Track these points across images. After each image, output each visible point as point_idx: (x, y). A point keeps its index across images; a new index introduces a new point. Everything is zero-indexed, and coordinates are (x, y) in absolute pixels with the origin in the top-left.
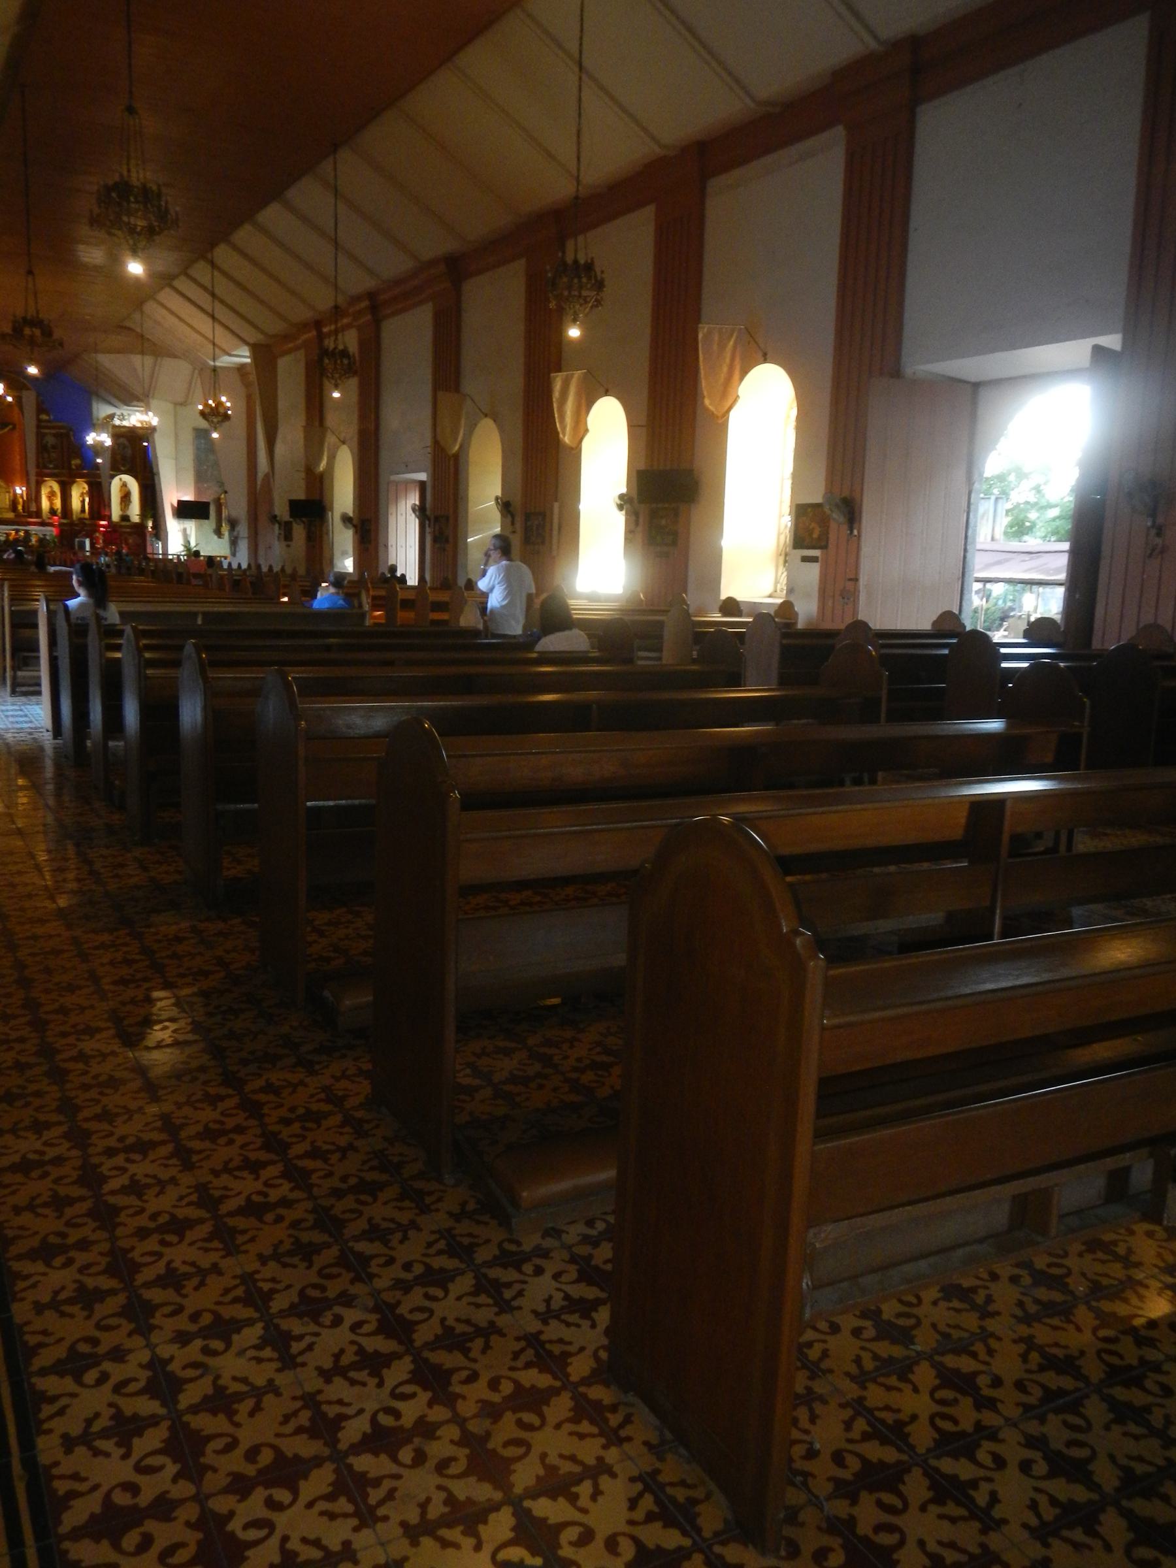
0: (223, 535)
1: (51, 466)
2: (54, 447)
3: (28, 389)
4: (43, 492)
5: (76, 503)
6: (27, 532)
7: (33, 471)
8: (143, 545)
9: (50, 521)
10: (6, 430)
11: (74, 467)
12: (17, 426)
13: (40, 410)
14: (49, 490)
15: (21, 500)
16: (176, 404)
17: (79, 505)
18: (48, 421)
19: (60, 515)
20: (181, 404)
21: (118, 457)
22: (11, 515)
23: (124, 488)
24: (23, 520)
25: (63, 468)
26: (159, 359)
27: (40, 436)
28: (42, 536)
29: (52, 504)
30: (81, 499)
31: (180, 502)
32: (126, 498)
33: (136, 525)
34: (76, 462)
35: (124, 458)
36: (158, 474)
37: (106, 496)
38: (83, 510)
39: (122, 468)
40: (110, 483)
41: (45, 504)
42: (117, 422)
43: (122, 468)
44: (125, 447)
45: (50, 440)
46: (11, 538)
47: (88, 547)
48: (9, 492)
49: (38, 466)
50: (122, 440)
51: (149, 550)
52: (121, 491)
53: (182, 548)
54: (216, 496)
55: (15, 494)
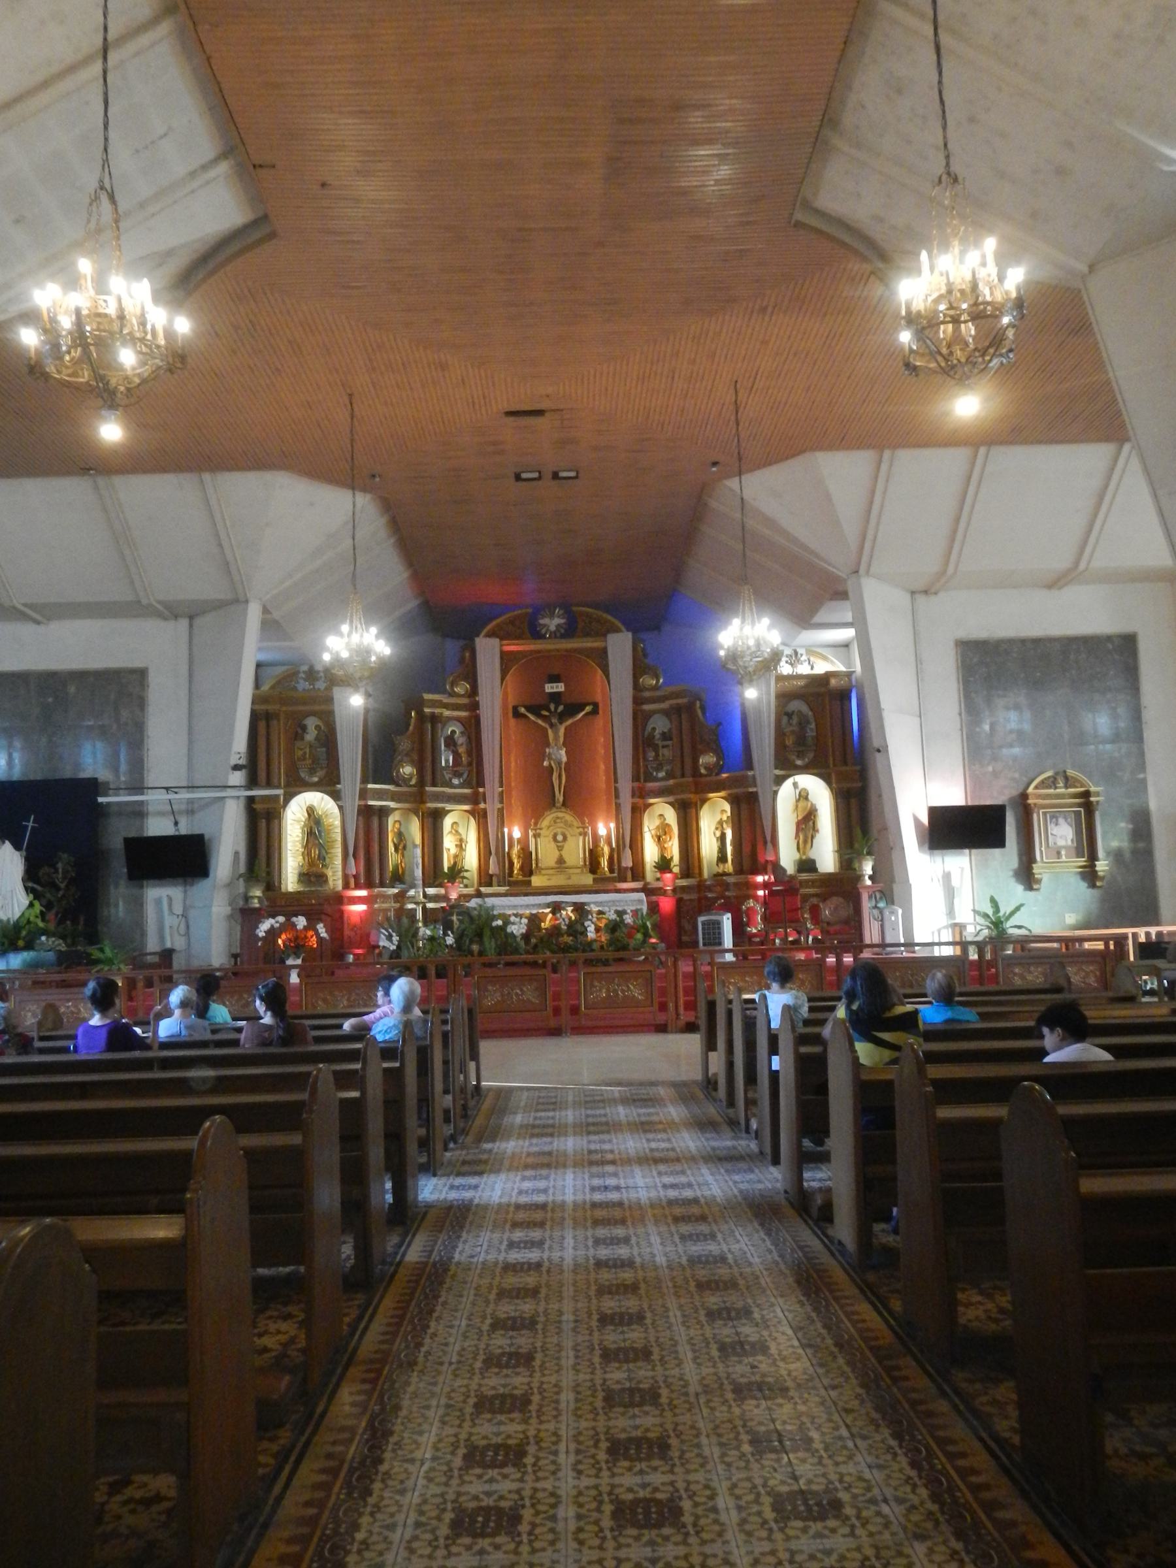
0: (1039, 881)
1: (661, 774)
2: (665, 736)
3: (618, 630)
4: (646, 829)
5: (708, 846)
6: (580, 908)
7: (626, 786)
8: (854, 922)
9: (659, 884)
11: (703, 771)
12: (601, 705)
13: (640, 667)
14: (657, 822)
15: (606, 850)
16: (913, 593)
17: (715, 846)
18: (656, 688)
19: (676, 870)
20: (926, 592)
21: (789, 741)
22: (588, 879)
23: (802, 804)
24: (611, 887)
25: (683, 776)
26: (887, 454)
27: (640, 719)
28: (613, 916)
29: (662, 849)
30: (718, 834)
31: (934, 812)
32: (807, 822)
33: (828, 879)
35: (801, 740)
36: (882, 750)
37: (767, 824)
38: (722, 858)
39: (799, 762)
40: (776, 793)
41: (651, 853)
42: (785, 669)
43: (799, 762)
45: (659, 725)
46: (546, 924)
47: (728, 941)
48: (585, 834)
49: (636, 778)
50: (797, 705)
51: (871, 934)
52: (797, 806)
53: (944, 921)
54: (1015, 792)
55: (596, 838)
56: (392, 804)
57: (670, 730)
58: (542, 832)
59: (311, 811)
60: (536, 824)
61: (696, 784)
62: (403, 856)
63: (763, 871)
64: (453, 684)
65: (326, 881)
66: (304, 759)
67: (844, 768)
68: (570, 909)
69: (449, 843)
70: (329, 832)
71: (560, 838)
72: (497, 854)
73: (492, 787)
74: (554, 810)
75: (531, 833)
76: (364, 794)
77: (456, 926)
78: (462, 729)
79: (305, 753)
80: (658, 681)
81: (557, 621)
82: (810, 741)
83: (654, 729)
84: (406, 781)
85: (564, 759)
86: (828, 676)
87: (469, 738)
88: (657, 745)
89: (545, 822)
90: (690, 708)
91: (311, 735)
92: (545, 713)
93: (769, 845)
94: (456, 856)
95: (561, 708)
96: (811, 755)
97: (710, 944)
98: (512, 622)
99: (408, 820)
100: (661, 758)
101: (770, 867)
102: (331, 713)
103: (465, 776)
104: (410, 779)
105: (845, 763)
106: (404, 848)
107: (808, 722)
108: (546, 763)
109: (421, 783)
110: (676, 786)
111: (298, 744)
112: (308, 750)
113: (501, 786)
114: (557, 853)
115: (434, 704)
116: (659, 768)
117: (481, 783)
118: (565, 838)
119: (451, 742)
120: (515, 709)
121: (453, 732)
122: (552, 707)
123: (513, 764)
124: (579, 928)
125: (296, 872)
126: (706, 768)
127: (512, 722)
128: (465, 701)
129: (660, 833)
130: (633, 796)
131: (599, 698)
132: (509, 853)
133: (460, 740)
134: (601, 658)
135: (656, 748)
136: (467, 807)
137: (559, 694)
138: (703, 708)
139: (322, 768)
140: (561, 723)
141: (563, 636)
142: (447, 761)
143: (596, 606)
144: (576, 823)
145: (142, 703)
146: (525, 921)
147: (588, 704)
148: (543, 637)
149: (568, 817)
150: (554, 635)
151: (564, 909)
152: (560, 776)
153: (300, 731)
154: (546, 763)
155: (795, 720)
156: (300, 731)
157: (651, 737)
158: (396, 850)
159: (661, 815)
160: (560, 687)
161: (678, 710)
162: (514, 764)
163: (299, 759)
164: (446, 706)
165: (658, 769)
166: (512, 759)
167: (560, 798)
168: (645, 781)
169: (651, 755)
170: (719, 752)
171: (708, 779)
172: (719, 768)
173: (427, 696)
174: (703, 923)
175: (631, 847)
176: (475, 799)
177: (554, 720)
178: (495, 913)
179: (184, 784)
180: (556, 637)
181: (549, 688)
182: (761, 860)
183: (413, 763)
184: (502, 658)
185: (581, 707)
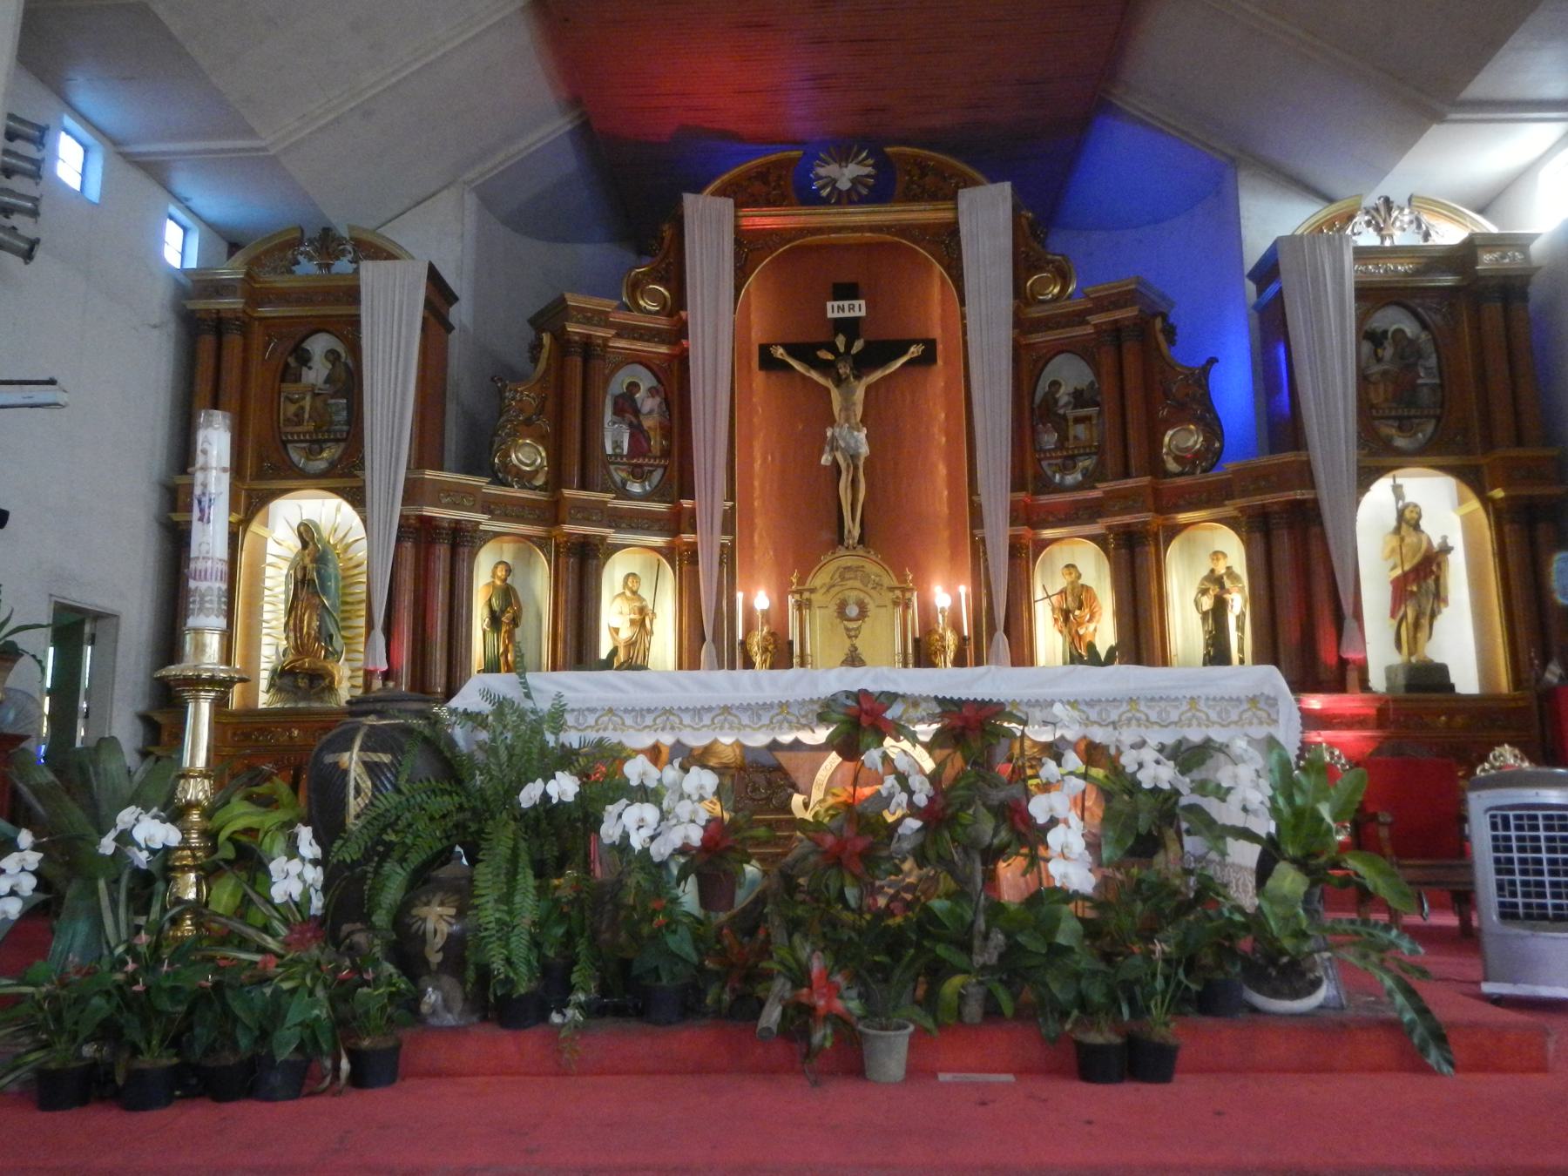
1: (1070, 479)
2: (1079, 398)
4: (1038, 593)
11: (1172, 466)
12: (940, 347)
13: (1025, 262)
14: (1060, 582)
15: (951, 639)
21: (1378, 396)
23: (1411, 539)
25: (1126, 474)
29: (1074, 638)
30: (1207, 603)
34: (1183, 439)
40: (1358, 503)
43: (1401, 442)
44: (1408, 352)
45: (1069, 374)
48: (907, 606)
49: (1018, 484)
52: (1402, 539)
56: (486, 523)
57: (1092, 383)
58: (817, 598)
59: (307, 533)
60: (801, 581)
61: (1157, 493)
62: (511, 635)
63: (1339, 686)
64: (636, 287)
65: (331, 688)
66: (300, 423)
67: (1514, 452)
68: (926, 731)
69: (614, 618)
70: (347, 581)
71: (853, 611)
72: (717, 639)
73: (709, 500)
74: (841, 551)
75: (791, 600)
76: (413, 492)
77: (354, 805)
78: (653, 382)
79: (302, 408)
80: (1063, 290)
82: (1425, 396)
83: (1055, 384)
84: (524, 479)
85: (864, 450)
86: (1470, 248)
87: (667, 401)
88: (1064, 417)
89: (820, 579)
90: (1142, 327)
91: (316, 373)
93: (1350, 623)
94: (631, 644)
95: (858, 346)
96: (1430, 428)
97: (1536, 917)
98: (762, 175)
99: (527, 560)
100: (1071, 444)
101: (1352, 677)
102: (355, 322)
103: (657, 476)
105: (1519, 441)
106: (515, 622)
107: (1420, 355)
108: (826, 460)
109: (557, 479)
110: (1110, 495)
111: (288, 388)
112: (307, 403)
113: (731, 497)
114: (848, 643)
115: (590, 317)
116: (1067, 465)
117: (687, 490)
118: (863, 614)
119: (626, 406)
120: (765, 350)
121: (634, 386)
122: (840, 341)
123: (757, 465)
124: (987, 829)
125: (269, 666)
126: (1177, 459)
127: (759, 378)
128: (662, 323)
129: (1071, 603)
130: (1012, 524)
131: (936, 333)
132: (743, 643)
133: (648, 404)
134: (946, 243)
135: (1061, 425)
136: (659, 541)
137: (857, 319)
138: (1170, 332)
139: (337, 441)
140: (858, 377)
141: (863, 201)
143: (931, 140)
144: (889, 580)
146: (703, 780)
147: (916, 342)
148: (825, 202)
149: (872, 568)
151: (899, 730)
152: (854, 483)
153: (291, 361)
154: (826, 460)
155: (1388, 352)
156: (291, 361)
157: (1051, 400)
158: (495, 620)
159: (1070, 567)
160: (857, 309)
161: (1117, 329)
162: (760, 462)
163: (288, 420)
164: (624, 331)
165: (1065, 469)
166: (758, 454)
167: (853, 529)
168: (1037, 492)
169: (1049, 439)
170: (1212, 426)
171: (1180, 481)
172: (1210, 456)
173: (573, 300)
174: (1499, 821)
175: (1007, 631)
176: (678, 523)
177: (844, 369)
178: (572, 738)
180: (851, 203)
181: (836, 310)
182: (1327, 654)
183: (541, 438)
184: (738, 242)
185: (900, 347)
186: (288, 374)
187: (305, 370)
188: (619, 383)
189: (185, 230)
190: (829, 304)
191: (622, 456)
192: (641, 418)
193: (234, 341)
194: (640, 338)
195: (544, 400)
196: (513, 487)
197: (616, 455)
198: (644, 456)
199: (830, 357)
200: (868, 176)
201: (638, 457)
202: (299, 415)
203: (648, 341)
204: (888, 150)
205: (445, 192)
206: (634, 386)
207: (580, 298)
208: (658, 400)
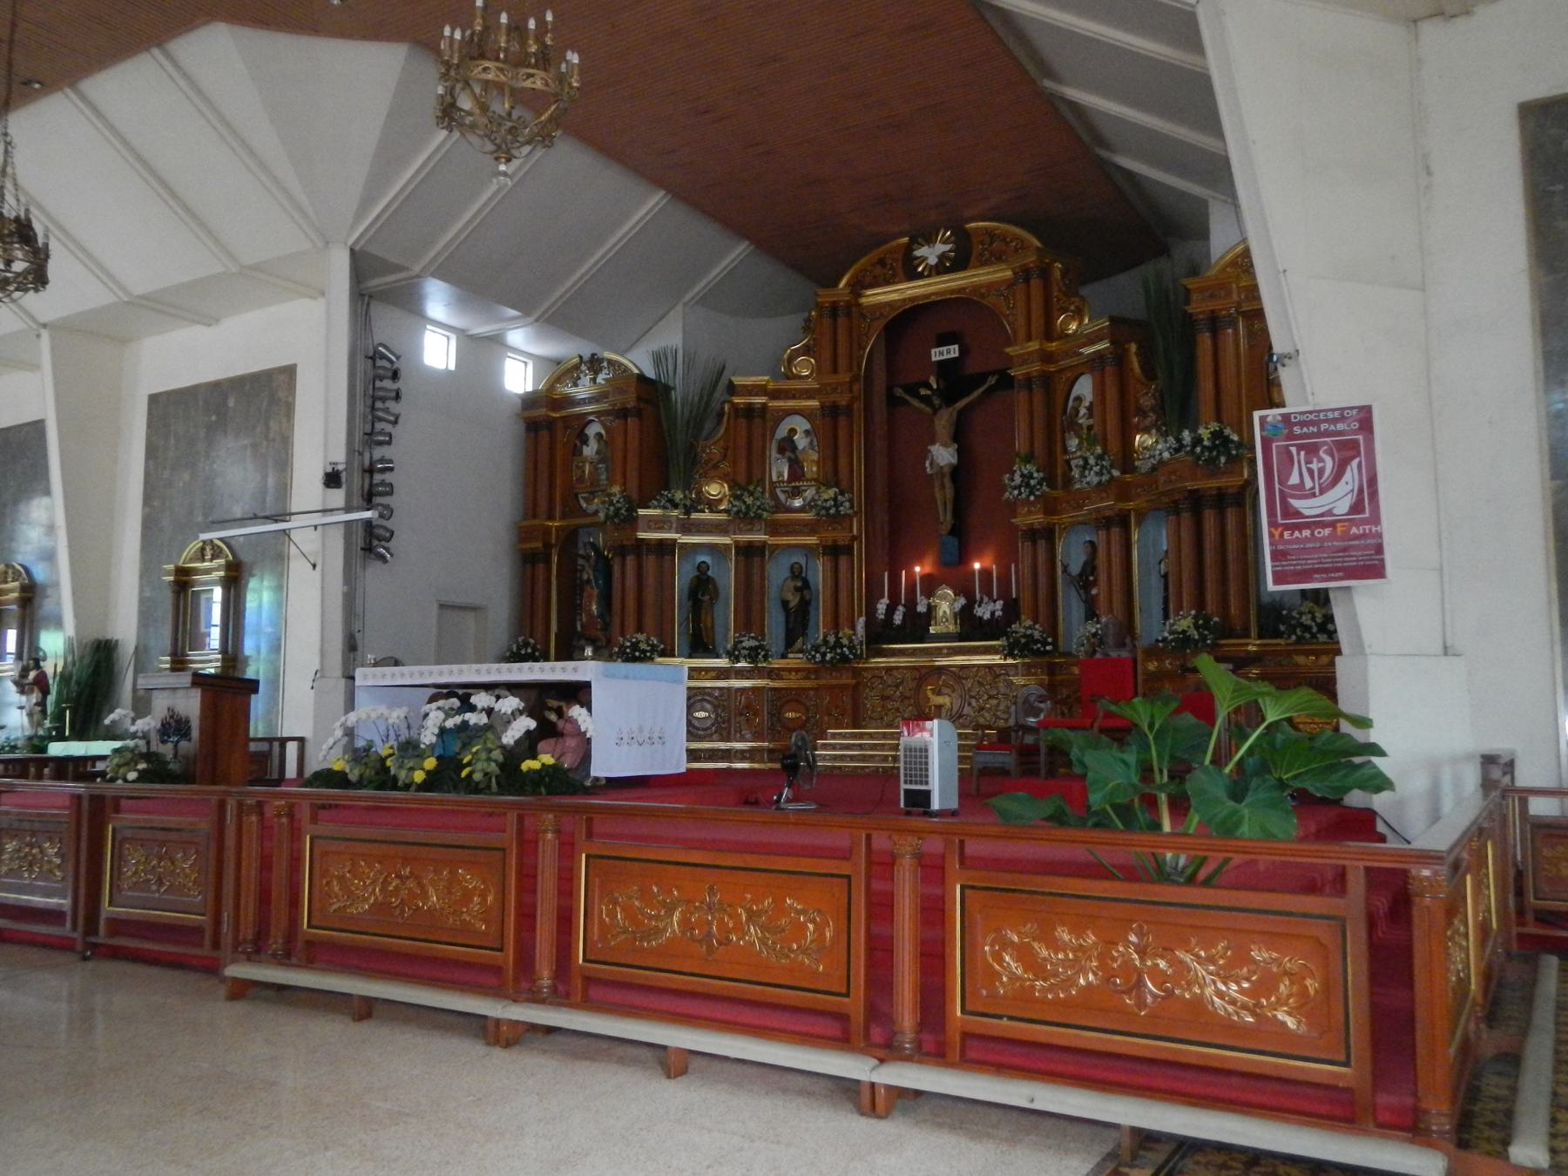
10: (976, 394)
78: (808, 426)
79: (584, 471)
81: (940, 248)
84: (712, 505)
88: (1081, 425)
92: (923, 392)
98: (881, 262)
104: (720, 501)
142: (780, 474)
145: (289, 409)
147: (992, 373)
148: (921, 276)
150: (939, 269)
153: (578, 444)
156: (578, 444)
160: (953, 351)
177: (937, 402)
179: (320, 508)
180: (939, 273)
185: (981, 378)
186: (577, 452)
187: (585, 447)
188: (782, 432)
189: (526, 363)
190: (933, 351)
191: (783, 482)
192: (798, 453)
193: (544, 434)
194: (794, 397)
195: (726, 449)
196: (704, 512)
197: (779, 482)
198: (799, 480)
199: (929, 392)
200: (950, 251)
201: (795, 481)
202: (581, 479)
203: (799, 398)
204: (968, 226)
205: (672, 313)
206: (793, 431)
207: (739, 379)
208: (808, 440)
